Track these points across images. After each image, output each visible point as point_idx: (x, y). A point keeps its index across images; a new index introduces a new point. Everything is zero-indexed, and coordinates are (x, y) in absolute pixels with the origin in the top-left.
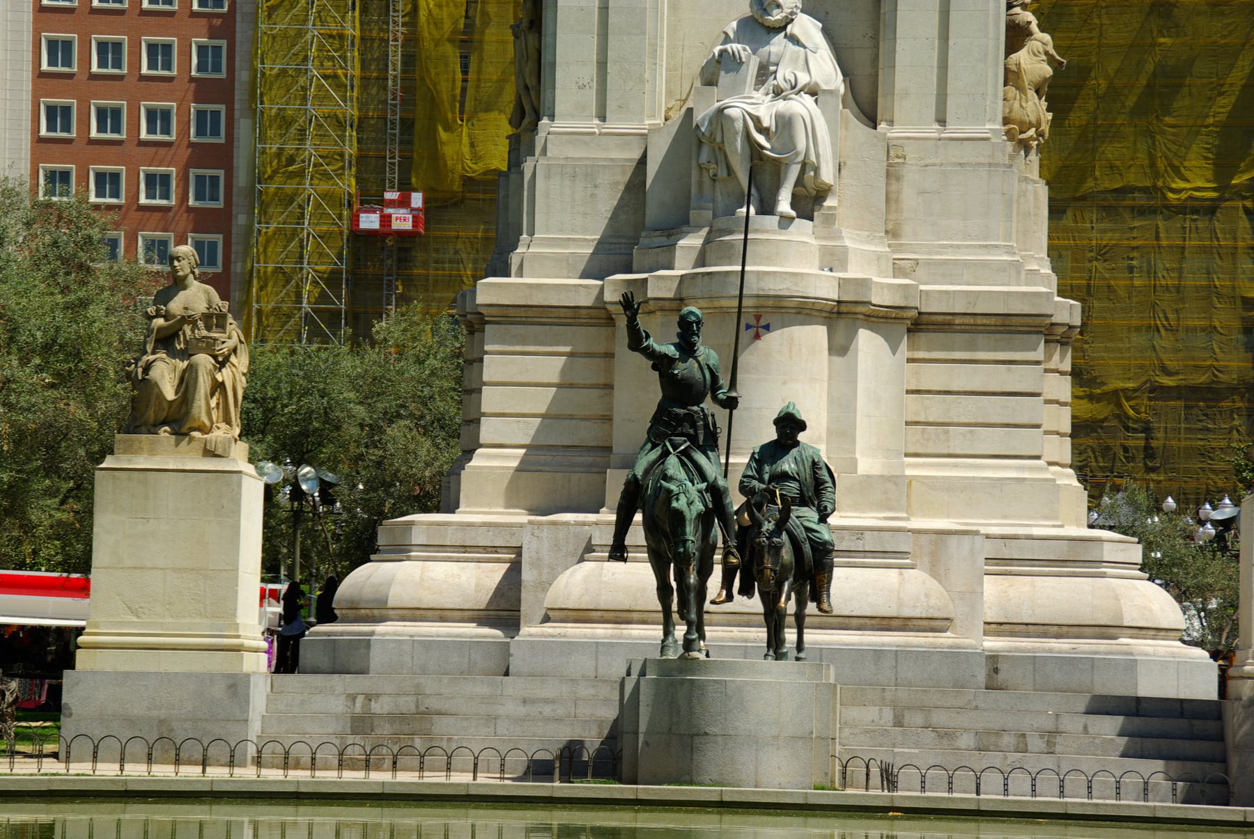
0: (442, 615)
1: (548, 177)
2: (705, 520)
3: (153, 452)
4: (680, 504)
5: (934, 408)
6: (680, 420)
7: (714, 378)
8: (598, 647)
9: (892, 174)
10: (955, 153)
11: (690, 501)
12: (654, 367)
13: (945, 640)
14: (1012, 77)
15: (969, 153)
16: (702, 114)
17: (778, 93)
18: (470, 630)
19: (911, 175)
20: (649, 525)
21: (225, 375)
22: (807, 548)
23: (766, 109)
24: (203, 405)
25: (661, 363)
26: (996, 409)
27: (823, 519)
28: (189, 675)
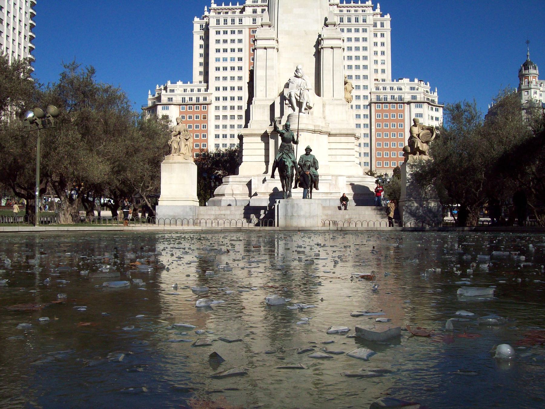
1: (255, 108)
2: (292, 167)
4: (287, 163)
5: (333, 152)
6: (285, 146)
7: (293, 137)
9: (324, 105)
10: (336, 102)
11: (289, 164)
12: (280, 136)
14: (346, 89)
15: (338, 102)
20: (279, 171)
21: (188, 143)
22: (313, 176)
24: (183, 149)
25: (282, 135)
26: (345, 152)
27: (316, 169)
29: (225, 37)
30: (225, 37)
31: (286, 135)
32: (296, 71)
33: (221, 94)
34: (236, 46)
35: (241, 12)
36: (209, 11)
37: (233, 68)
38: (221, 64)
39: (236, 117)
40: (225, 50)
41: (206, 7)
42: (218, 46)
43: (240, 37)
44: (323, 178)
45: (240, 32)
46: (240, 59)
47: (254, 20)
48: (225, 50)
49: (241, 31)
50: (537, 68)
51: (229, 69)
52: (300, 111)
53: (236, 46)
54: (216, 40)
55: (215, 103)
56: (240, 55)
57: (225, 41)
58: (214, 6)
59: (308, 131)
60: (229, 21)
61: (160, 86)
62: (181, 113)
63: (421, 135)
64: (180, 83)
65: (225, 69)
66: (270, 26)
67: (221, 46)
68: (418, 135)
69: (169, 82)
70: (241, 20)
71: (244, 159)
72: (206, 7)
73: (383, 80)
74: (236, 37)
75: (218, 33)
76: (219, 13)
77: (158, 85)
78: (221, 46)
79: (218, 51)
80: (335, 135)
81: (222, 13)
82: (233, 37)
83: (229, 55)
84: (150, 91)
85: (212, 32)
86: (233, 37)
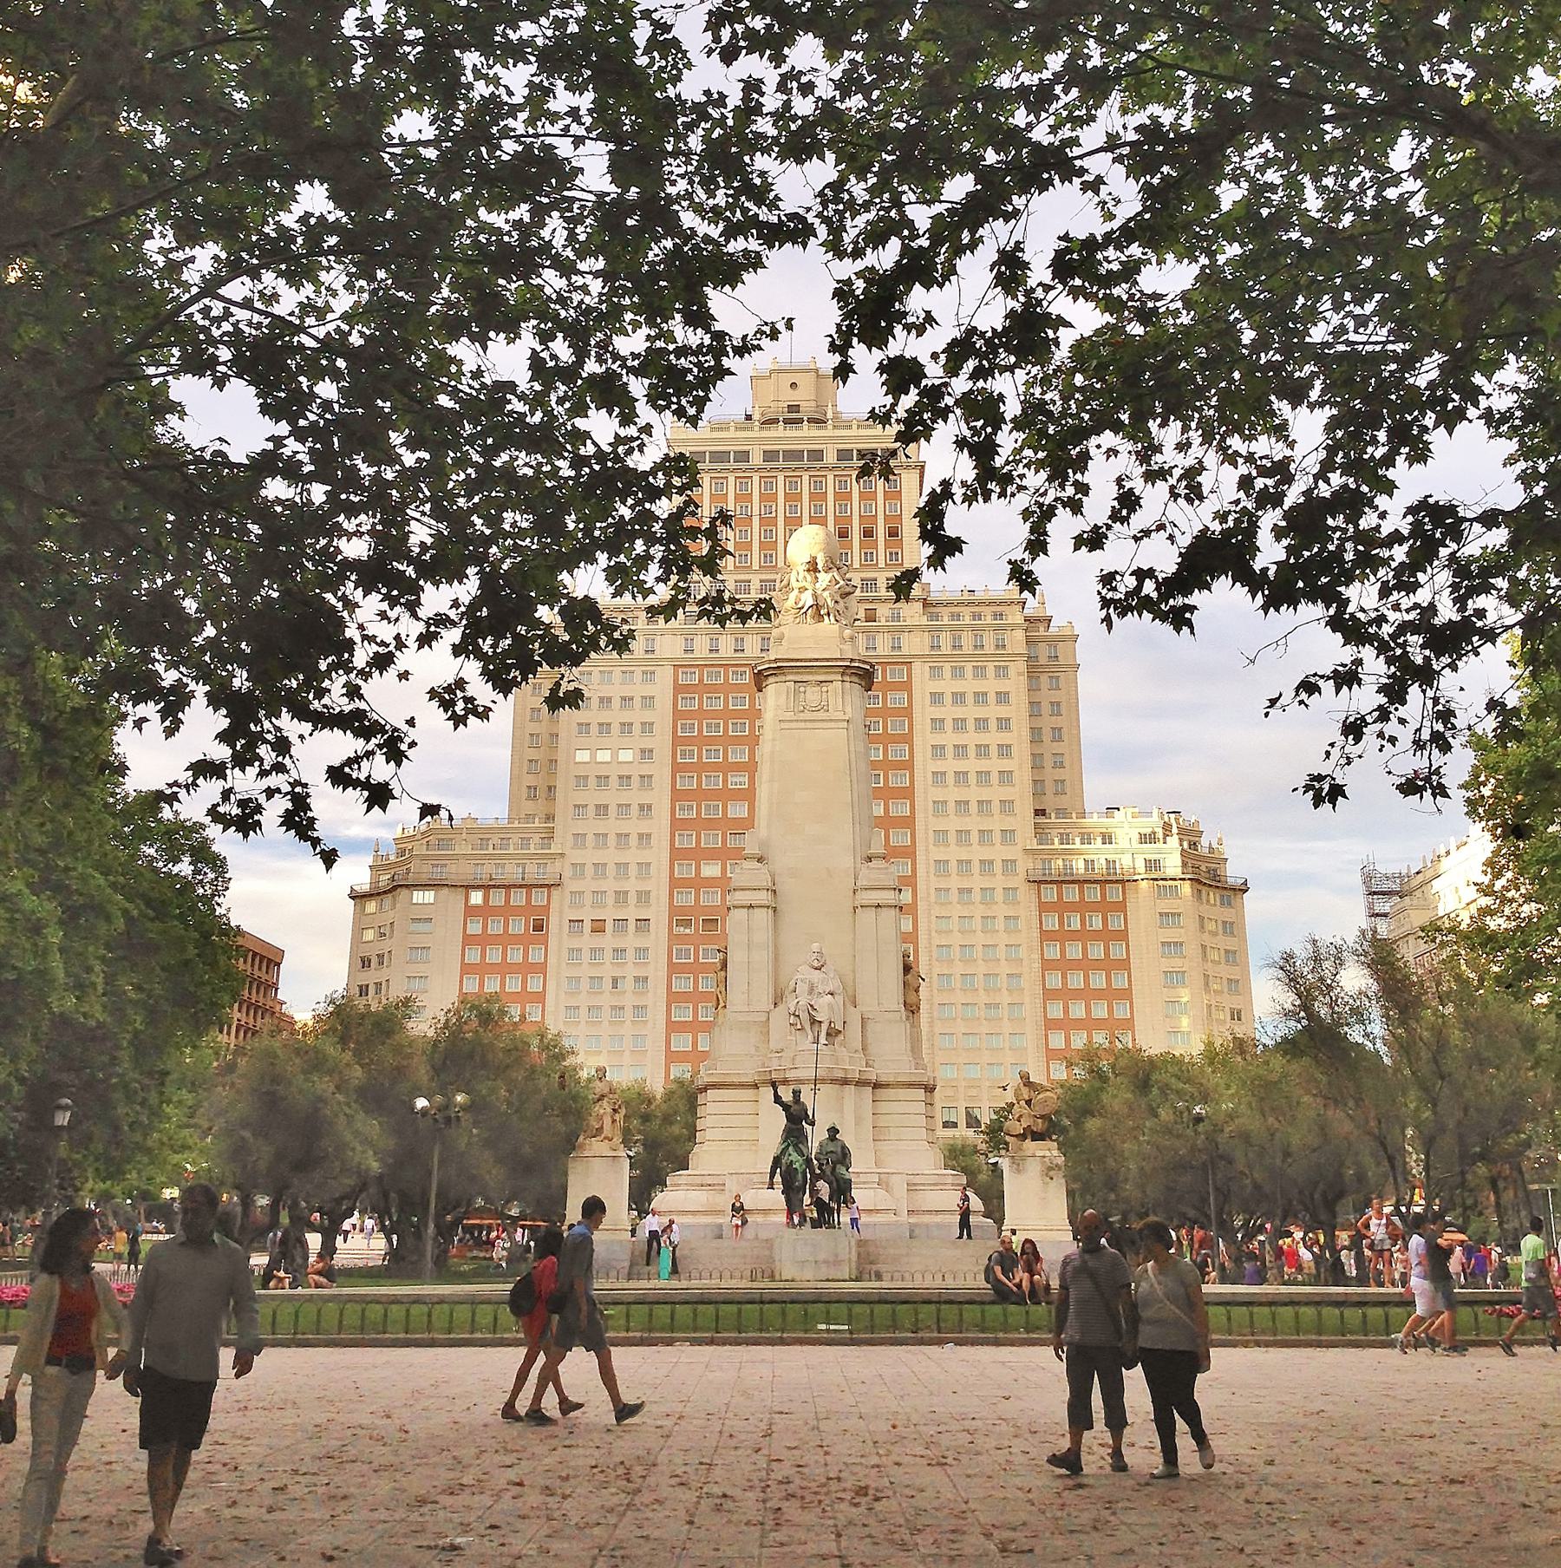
0: (694, 1213)
4: (796, 1166)
11: (798, 1162)
13: (891, 1218)
19: (870, 1026)
25: (786, 1107)
31: (795, 1108)
33: (589, 856)
39: (632, 925)
43: (648, 690)
44: (863, 1178)
48: (605, 727)
53: (636, 716)
55: (571, 885)
56: (647, 743)
59: (833, 1081)
62: (471, 911)
66: (760, 860)
71: (709, 1134)
73: (1061, 812)
80: (887, 1086)
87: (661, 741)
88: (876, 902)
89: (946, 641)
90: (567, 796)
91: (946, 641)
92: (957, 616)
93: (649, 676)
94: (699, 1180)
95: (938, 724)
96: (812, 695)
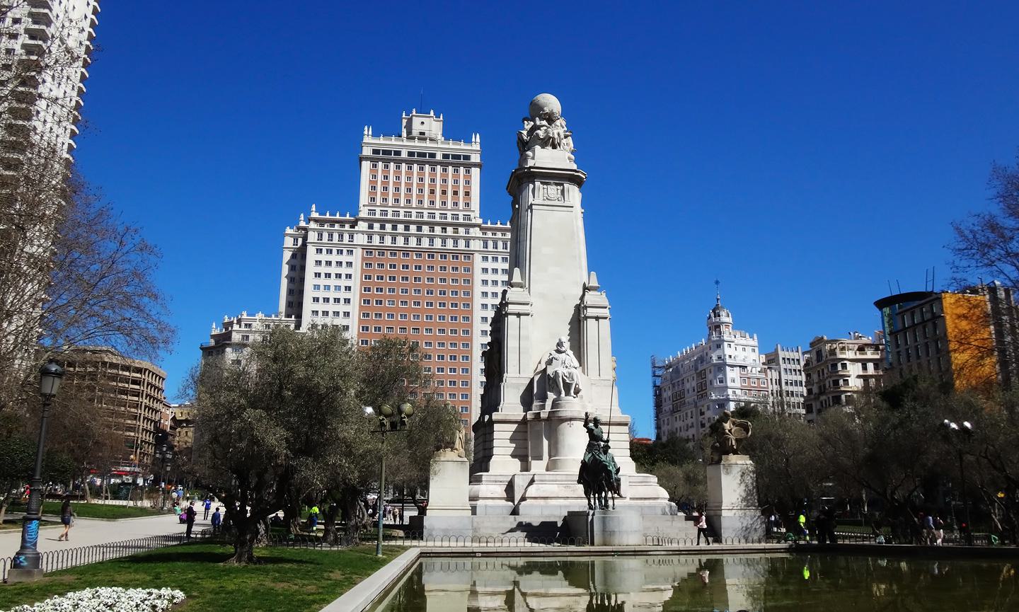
3: (445, 457)
8: (542, 507)
16: (550, 371)
17: (567, 367)
18: (504, 502)
23: (566, 371)
25: (590, 431)
28: (458, 517)
29: (329, 258)
30: (329, 258)
31: (596, 431)
32: (558, 345)
34: (344, 270)
35: (352, 227)
36: (309, 220)
37: (337, 300)
38: (321, 294)
40: (328, 275)
41: (302, 215)
42: (318, 270)
43: (350, 259)
45: (350, 252)
46: (348, 288)
47: (370, 238)
48: (328, 275)
49: (352, 251)
50: (730, 315)
51: (332, 301)
52: (568, 394)
53: (344, 270)
54: (316, 261)
57: (329, 263)
58: (315, 215)
60: (336, 236)
61: (230, 318)
63: (733, 431)
64: (260, 316)
65: (326, 300)
67: (323, 269)
68: (730, 431)
69: (245, 313)
70: (351, 237)
71: (495, 451)
72: (302, 215)
74: (344, 258)
75: (319, 251)
76: (322, 225)
77: (226, 317)
78: (323, 269)
79: (318, 275)
81: (326, 226)
82: (339, 258)
83: (333, 282)
84: (214, 324)
85: (311, 250)
86: (339, 258)
87: (355, 283)
88: (595, 315)
89: (490, 244)
90: (308, 306)
91: (490, 244)
92: (495, 234)
93: (350, 252)
94: (493, 478)
95: (485, 282)
96: (553, 190)
